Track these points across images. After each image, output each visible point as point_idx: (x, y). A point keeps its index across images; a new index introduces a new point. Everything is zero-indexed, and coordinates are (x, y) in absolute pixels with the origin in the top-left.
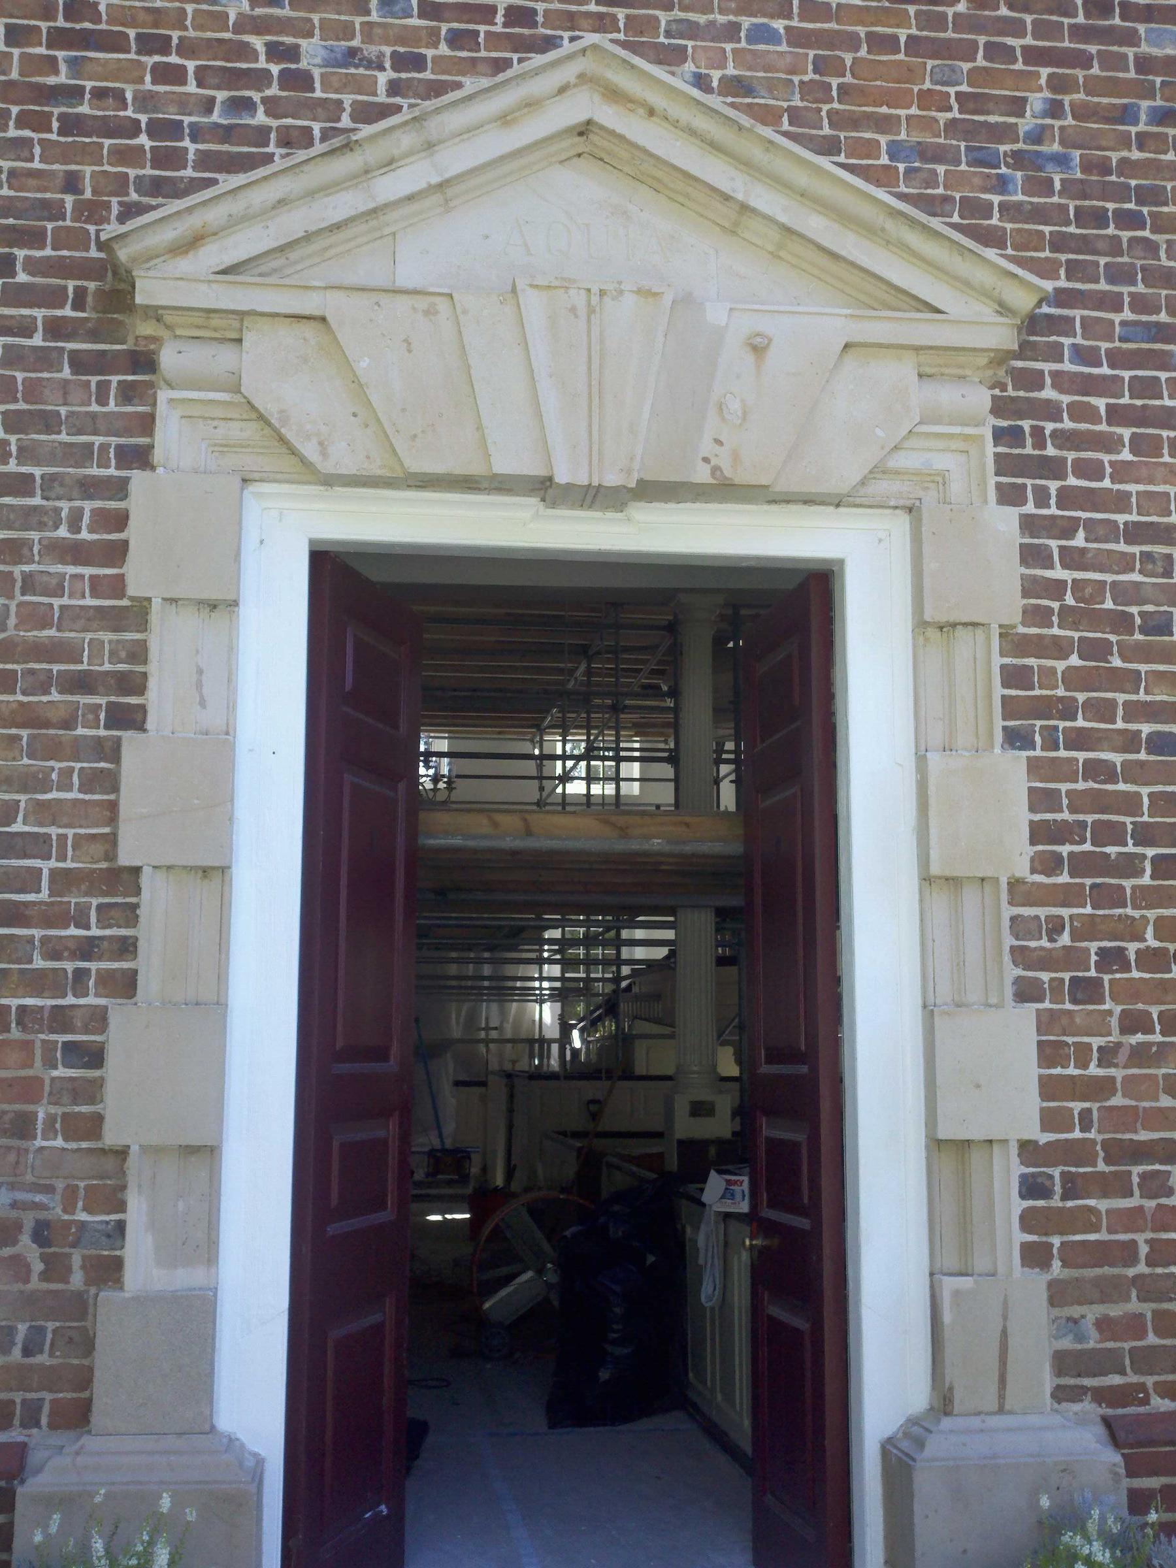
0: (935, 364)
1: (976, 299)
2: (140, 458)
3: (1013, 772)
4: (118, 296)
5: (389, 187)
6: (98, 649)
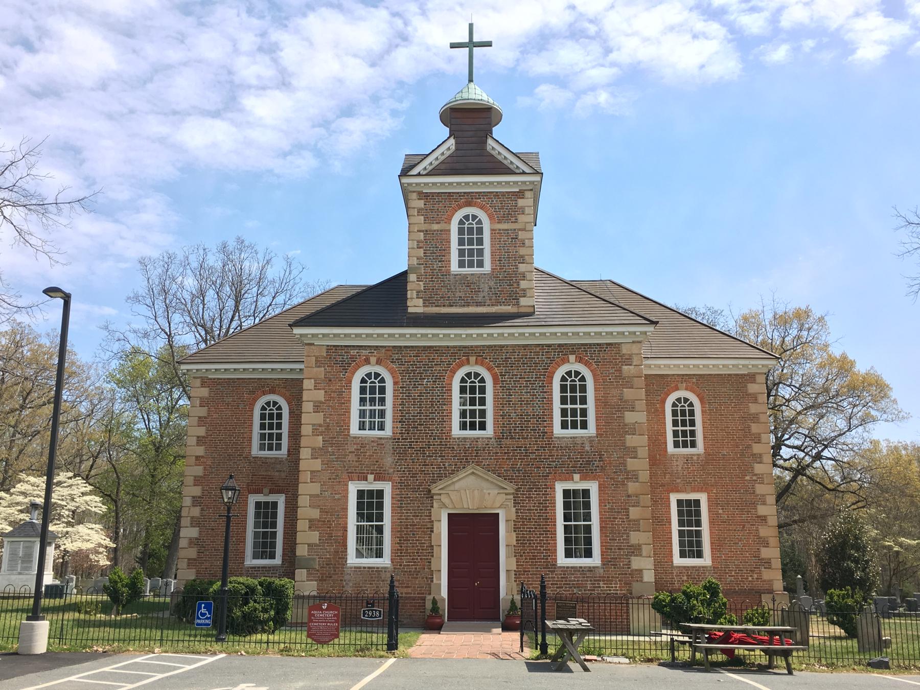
0: (506, 494)
1: (510, 488)
2: (432, 507)
3: (514, 535)
4: (430, 491)
5: (454, 480)
6: (429, 525)
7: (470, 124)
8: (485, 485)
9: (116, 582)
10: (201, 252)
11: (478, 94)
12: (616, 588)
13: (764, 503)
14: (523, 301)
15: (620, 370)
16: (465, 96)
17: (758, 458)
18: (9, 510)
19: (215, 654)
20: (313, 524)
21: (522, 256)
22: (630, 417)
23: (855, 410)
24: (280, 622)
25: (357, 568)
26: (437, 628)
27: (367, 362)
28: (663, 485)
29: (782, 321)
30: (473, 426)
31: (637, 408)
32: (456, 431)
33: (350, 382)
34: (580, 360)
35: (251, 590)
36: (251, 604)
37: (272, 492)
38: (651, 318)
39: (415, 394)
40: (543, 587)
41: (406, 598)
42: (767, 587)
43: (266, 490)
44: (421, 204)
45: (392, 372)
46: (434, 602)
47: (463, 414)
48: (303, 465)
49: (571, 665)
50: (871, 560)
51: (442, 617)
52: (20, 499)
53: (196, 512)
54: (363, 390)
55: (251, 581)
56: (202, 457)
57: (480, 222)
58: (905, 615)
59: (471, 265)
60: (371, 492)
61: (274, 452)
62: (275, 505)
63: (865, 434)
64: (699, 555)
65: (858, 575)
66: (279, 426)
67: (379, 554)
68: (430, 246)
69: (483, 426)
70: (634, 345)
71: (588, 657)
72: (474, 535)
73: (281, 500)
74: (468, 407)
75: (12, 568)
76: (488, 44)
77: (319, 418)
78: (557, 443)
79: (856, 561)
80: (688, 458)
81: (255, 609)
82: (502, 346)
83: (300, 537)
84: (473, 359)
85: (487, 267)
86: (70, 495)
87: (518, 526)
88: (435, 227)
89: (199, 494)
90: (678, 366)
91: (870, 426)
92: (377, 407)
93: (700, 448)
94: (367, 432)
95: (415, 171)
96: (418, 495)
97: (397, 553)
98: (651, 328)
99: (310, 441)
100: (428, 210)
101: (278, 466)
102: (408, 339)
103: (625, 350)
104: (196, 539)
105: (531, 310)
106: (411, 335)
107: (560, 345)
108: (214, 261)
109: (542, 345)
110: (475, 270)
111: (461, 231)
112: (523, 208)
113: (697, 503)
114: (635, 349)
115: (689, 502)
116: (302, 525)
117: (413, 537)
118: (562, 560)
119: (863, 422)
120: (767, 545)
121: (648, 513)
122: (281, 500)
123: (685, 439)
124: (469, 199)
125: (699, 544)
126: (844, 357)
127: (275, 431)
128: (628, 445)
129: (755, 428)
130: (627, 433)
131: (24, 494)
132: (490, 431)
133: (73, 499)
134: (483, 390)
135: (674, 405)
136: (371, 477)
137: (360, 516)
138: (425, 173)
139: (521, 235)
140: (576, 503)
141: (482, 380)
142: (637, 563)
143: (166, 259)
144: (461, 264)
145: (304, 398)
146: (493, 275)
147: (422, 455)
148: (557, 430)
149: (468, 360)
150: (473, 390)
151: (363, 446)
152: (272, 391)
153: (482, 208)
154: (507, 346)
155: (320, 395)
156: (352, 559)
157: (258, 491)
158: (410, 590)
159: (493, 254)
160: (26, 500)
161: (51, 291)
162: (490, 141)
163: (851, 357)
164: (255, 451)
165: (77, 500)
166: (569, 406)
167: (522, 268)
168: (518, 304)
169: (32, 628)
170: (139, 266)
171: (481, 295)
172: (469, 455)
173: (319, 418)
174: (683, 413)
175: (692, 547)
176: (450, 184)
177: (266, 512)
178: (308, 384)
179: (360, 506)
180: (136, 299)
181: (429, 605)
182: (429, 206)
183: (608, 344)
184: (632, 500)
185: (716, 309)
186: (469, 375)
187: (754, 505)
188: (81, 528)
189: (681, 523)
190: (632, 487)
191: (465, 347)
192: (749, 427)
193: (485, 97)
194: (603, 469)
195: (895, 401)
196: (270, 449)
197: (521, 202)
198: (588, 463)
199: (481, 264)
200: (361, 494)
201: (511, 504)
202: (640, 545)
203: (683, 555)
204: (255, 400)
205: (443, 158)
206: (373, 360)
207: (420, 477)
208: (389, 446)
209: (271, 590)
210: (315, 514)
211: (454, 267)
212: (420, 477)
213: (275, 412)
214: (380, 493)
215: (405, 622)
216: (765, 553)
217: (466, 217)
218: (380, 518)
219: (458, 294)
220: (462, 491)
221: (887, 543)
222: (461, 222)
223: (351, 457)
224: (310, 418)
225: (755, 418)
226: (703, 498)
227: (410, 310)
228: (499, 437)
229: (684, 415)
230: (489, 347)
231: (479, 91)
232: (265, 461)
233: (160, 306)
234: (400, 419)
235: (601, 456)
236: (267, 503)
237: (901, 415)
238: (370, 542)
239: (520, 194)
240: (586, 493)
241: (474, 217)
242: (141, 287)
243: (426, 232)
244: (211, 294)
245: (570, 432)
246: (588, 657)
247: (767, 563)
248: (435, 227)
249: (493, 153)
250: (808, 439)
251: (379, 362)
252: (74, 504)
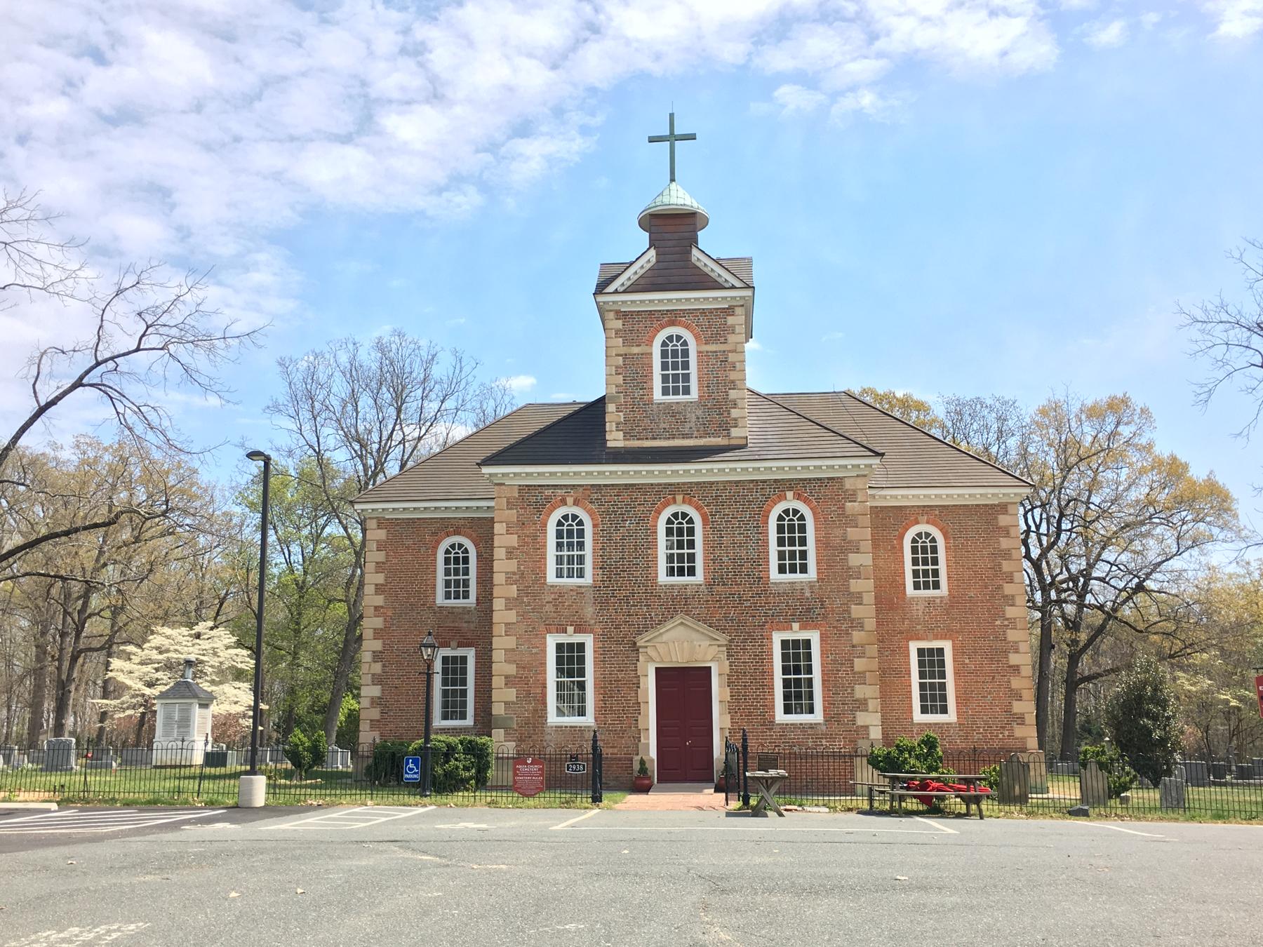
1: (723, 639)
7: (673, 230)
8: (694, 635)
9: (297, 745)
10: (351, 346)
11: (680, 197)
12: (840, 745)
13: (1017, 651)
14: (735, 432)
15: (843, 508)
16: (666, 200)
17: (1010, 600)
18: (145, 669)
19: (425, 806)
20: (509, 681)
21: (733, 382)
22: (854, 560)
23: (1185, 527)
24: (481, 782)
25: (559, 728)
26: (645, 789)
27: (564, 502)
28: (901, 632)
29: (1094, 413)
30: (681, 572)
31: (862, 549)
32: (663, 578)
33: (545, 525)
34: (798, 497)
35: (451, 749)
36: (453, 762)
37: (460, 645)
38: (877, 449)
39: (617, 537)
40: (745, 740)
41: (612, 759)
42: (1019, 745)
43: (454, 644)
44: (619, 324)
45: (591, 514)
46: (642, 762)
47: (670, 558)
48: (496, 617)
49: (769, 813)
50: (1174, 716)
51: (650, 778)
52: (155, 655)
53: (377, 668)
54: (559, 534)
55: (453, 740)
57: (685, 343)
58: (1232, 785)
59: (676, 392)
60: (571, 646)
62: (464, 659)
63: (1202, 558)
64: (944, 710)
65: (1156, 735)
66: (466, 572)
67: (582, 712)
68: (631, 371)
69: (692, 572)
70: (859, 480)
71: (788, 807)
72: (684, 690)
73: (470, 654)
74: (675, 551)
75: (167, 734)
76: (692, 137)
77: (512, 566)
78: (774, 589)
79: (1155, 718)
80: (930, 602)
81: (457, 767)
82: (712, 483)
83: (496, 696)
84: (679, 498)
85: (694, 394)
86: (214, 648)
87: (731, 681)
88: (636, 350)
89: (380, 648)
90: (918, 496)
91: (1209, 546)
92: (575, 553)
93: (944, 590)
94: (565, 581)
95: (611, 288)
96: (622, 648)
97: (601, 711)
98: (876, 461)
99: (503, 591)
100: (629, 328)
102: (607, 477)
103: (848, 485)
105: (743, 442)
106: (611, 472)
107: (776, 481)
108: (369, 359)
109: (757, 481)
110: (681, 398)
111: (664, 354)
112: (733, 327)
113: (941, 651)
114: (859, 484)
115: (931, 651)
116: (497, 682)
117: (618, 692)
118: (780, 717)
119: (1195, 543)
120: (1020, 698)
121: (874, 665)
122: (470, 654)
123: (927, 580)
124: (673, 318)
125: (944, 698)
126: (1174, 459)
127: (461, 577)
128: (852, 590)
129: (1006, 566)
130: (851, 577)
131: (160, 650)
132: (699, 577)
133: (215, 654)
134: (691, 532)
135: (914, 541)
136: (570, 629)
137: (560, 671)
138: (621, 289)
140: (796, 655)
141: (691, 521)
142: (862, 719)
143: (312, 358)
144: (665, 391)
145: (496, 544)
146: (700, 403)
147: (627, 604)
148: (774, 575)
149: (674, 499)
150: (680, 532)
151: (561, 595)
152: (457, 533)
153: (687, 327)
154: (717, 482)
155: (513, 540)
156: (553, 718)
157: (445, 645)
158: (615, 751)
159: (700, 380)
160: (160, 657)
161: (253, 455)
162: (694, 251)
163: (1183, 458)
164: (440, 600)
165: (221, 654)
166: (787, 548)
167: (733, 394)
169: (251, 781)
170: (279, 369)
171: (687, 425)
172: (678, 604)
173: (512, 566)
174: (924, 550)
175: (934, 700)
176: (651, 301)
177: (454, 669)
178: (499, 528)
179: (559, 660)
180: (276, 408)
181: (636, 766)
182: (628, 327)
183: (829, 479)
184: (858, 650)
185: (1006, 399)
186: (675, 515)
187: (1006, 653)
188: (227, 688)
189: (922, 675)
190: (857, 636)
191: (670, 485)
192: (1000, 564)
193: (688, 202)
194: (825, 617)
195: (1236, 516)
196: (457, 597)
197: (730, 320)
198: (809, 610)
199: (687, 391)
200: (560, 647)
201: (724, 656)
202: (866, 700)
203: (924, 710)
204: (438, 542)
205: (643, 271)
206: (570, 500)
207: (625, 628)
208: (590, 595)
209: (471, 748)
210: (511, 669)
211: (657, 395)
212: (625, 628)
214: (581, 646)
215: (612, 784)
216: (1018, 707)
217: (670, 338)
218: (582, 673)
219: (662, 425)
220: (671, 644)
221: (1223, 697)
222: (664, 344)
224: (503, 566)
225: (1007, 555)
226: (947, 646)
227: (609, 444)
228: (709, 585)
229: (925, 552)
231: (681, 192)
232: (451, 611)
233: (305, 415)
234: (601, 566)
235: (822, 602)
236: (454, 658)
237: (1243, 534)
238: (572, 699)
239: (730, 311)
240: (807, 643)
241: (679, 338)
242: (281, 392)
243: (625, 356)
244: (365, 401)
245: (788, 577)
246: (788, 807)
247: (1020, 719)
248: (636, 350)
249: (698, 264)
250: (1114, 568)
251: (576, 503)
252: (216, 659)
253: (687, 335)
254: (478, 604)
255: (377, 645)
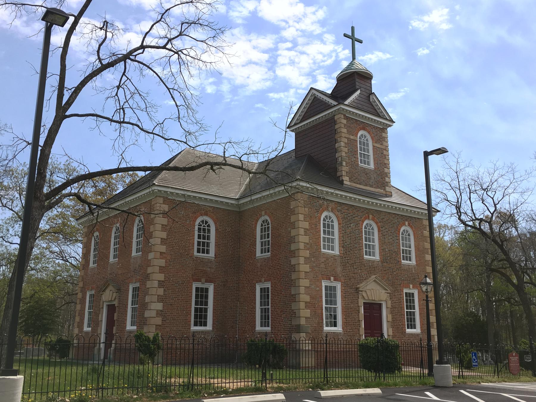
0: (388, 293)
2: (358, 298)
4: (357, 288)
15: (422, 233)
43: (203, 280)
56: (164, 253)
61: (205, 255)
88: (352, 137)
101: (209, 264)
104: (161, 311)
107: (402, 215)
139: (385, 153)
147: (351, 267)
149: (369, 216)
151: (327, 259)
152: (206, 214)
153: (369, 133)
157: (198, 280)
168: (385, 190)
171: (371, 181)
191: (367, 209)
196: (203, 252)
201: (388, 299)
204: (196, 218)
210: (307, 298)
213: (206, 228)
223: (322, 265)
230: (376, 210)
234: (342, 245)
253: (368, 137)
254: (215, 258)
255: (161, 277)
